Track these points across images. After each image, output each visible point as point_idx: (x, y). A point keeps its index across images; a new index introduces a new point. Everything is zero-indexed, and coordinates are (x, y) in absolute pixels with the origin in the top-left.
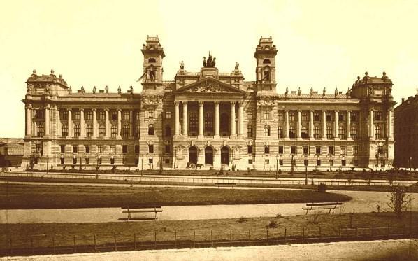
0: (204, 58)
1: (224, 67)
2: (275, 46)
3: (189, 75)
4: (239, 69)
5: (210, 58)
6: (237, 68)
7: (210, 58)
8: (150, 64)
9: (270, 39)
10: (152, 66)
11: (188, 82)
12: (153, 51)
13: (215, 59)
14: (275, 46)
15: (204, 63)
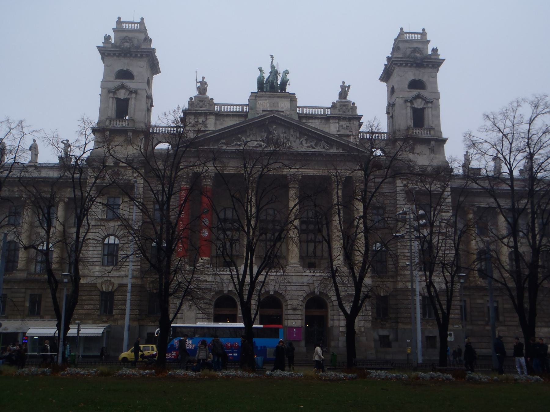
0: (260, 69)
1: (312, 94)
2: (435, 50)
3: (217, 108)
4: (350, 98)
5: (274, 73)
6: (344, 92)
7: (274, 73)
8: (118, 82)
9: (423, 33)
10: (123, 87)
11: (212, 125)
12: (129, 55)
13: (286, 73)
14: (435, 50)
15: (261, 84)
